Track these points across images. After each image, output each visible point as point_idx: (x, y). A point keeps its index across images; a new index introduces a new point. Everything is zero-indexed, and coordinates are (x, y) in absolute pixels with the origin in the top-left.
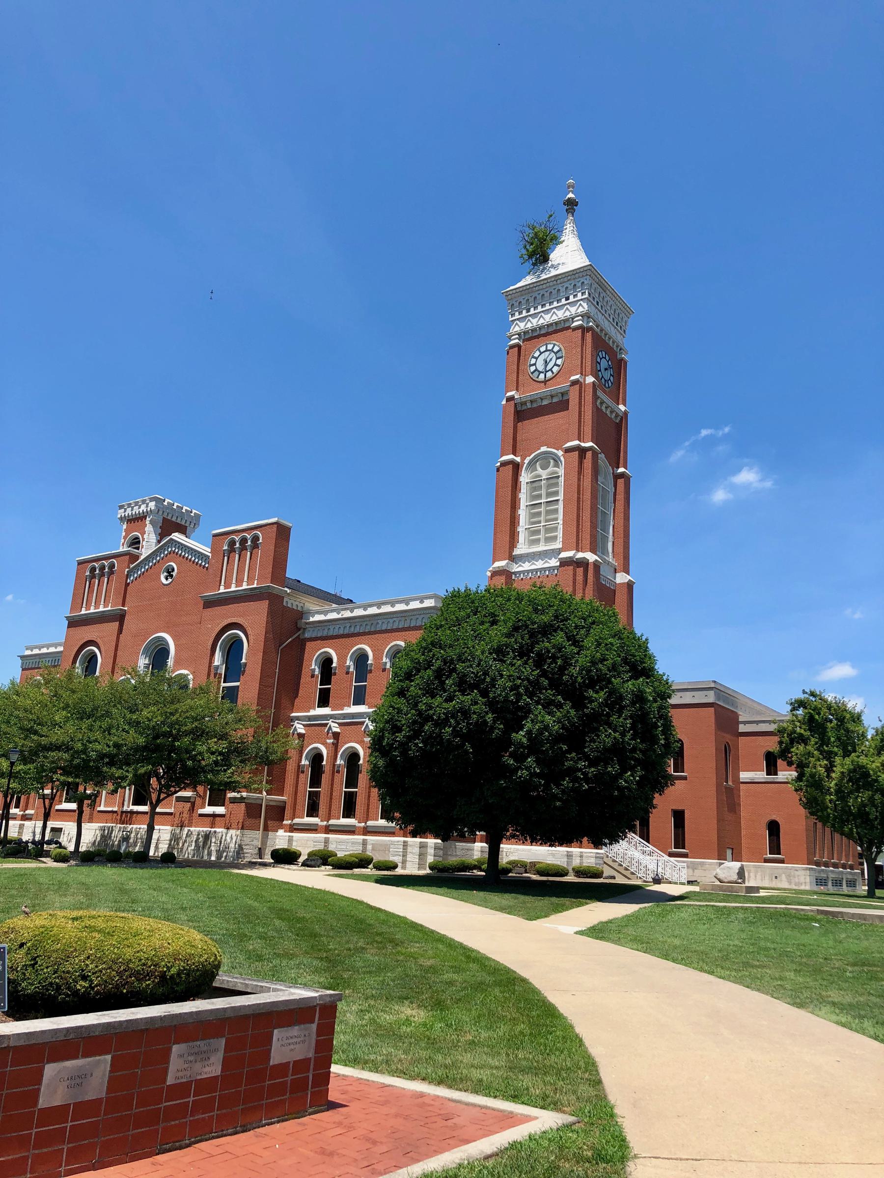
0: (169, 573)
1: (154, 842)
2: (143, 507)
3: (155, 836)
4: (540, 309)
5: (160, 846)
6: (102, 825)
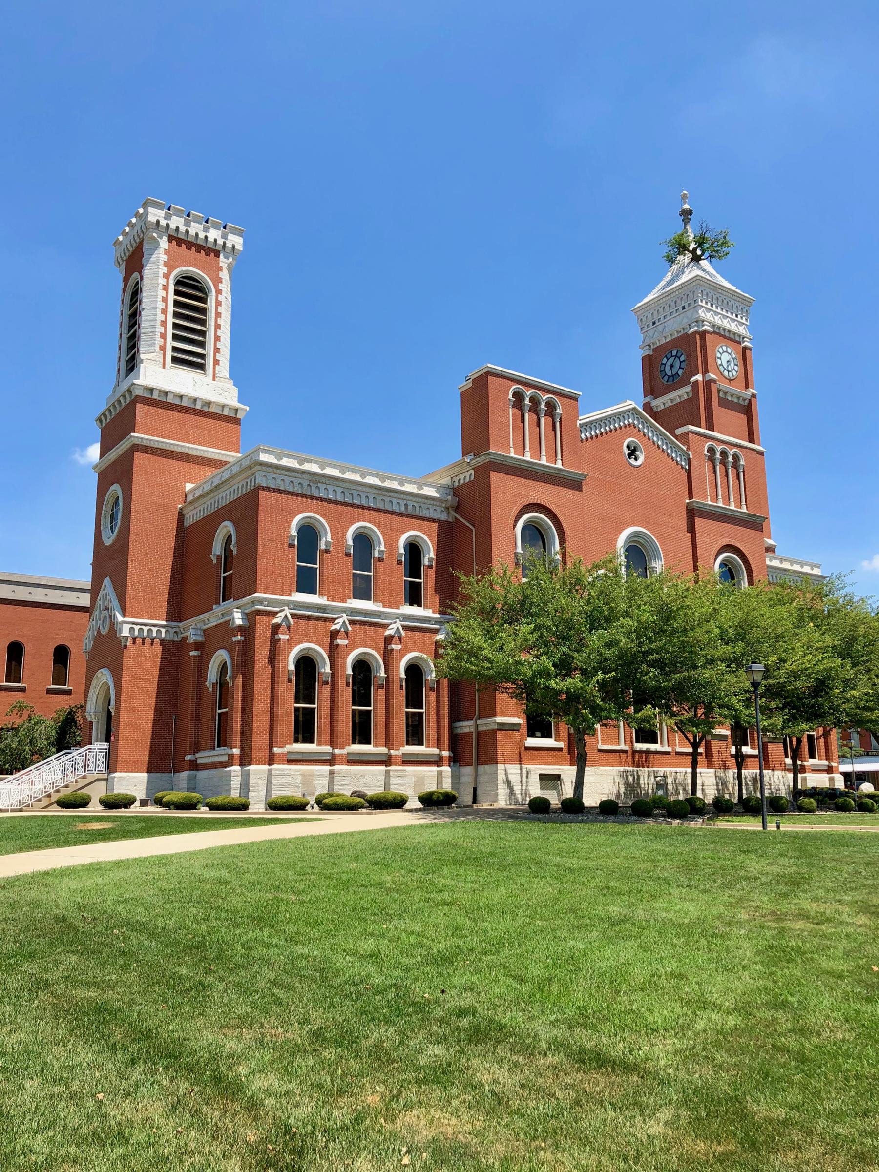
0: (633, 452)
1: (699, 787)
2: (214, 235)
4: (719, 311)
5: (707, 791)
6: (622, 769)
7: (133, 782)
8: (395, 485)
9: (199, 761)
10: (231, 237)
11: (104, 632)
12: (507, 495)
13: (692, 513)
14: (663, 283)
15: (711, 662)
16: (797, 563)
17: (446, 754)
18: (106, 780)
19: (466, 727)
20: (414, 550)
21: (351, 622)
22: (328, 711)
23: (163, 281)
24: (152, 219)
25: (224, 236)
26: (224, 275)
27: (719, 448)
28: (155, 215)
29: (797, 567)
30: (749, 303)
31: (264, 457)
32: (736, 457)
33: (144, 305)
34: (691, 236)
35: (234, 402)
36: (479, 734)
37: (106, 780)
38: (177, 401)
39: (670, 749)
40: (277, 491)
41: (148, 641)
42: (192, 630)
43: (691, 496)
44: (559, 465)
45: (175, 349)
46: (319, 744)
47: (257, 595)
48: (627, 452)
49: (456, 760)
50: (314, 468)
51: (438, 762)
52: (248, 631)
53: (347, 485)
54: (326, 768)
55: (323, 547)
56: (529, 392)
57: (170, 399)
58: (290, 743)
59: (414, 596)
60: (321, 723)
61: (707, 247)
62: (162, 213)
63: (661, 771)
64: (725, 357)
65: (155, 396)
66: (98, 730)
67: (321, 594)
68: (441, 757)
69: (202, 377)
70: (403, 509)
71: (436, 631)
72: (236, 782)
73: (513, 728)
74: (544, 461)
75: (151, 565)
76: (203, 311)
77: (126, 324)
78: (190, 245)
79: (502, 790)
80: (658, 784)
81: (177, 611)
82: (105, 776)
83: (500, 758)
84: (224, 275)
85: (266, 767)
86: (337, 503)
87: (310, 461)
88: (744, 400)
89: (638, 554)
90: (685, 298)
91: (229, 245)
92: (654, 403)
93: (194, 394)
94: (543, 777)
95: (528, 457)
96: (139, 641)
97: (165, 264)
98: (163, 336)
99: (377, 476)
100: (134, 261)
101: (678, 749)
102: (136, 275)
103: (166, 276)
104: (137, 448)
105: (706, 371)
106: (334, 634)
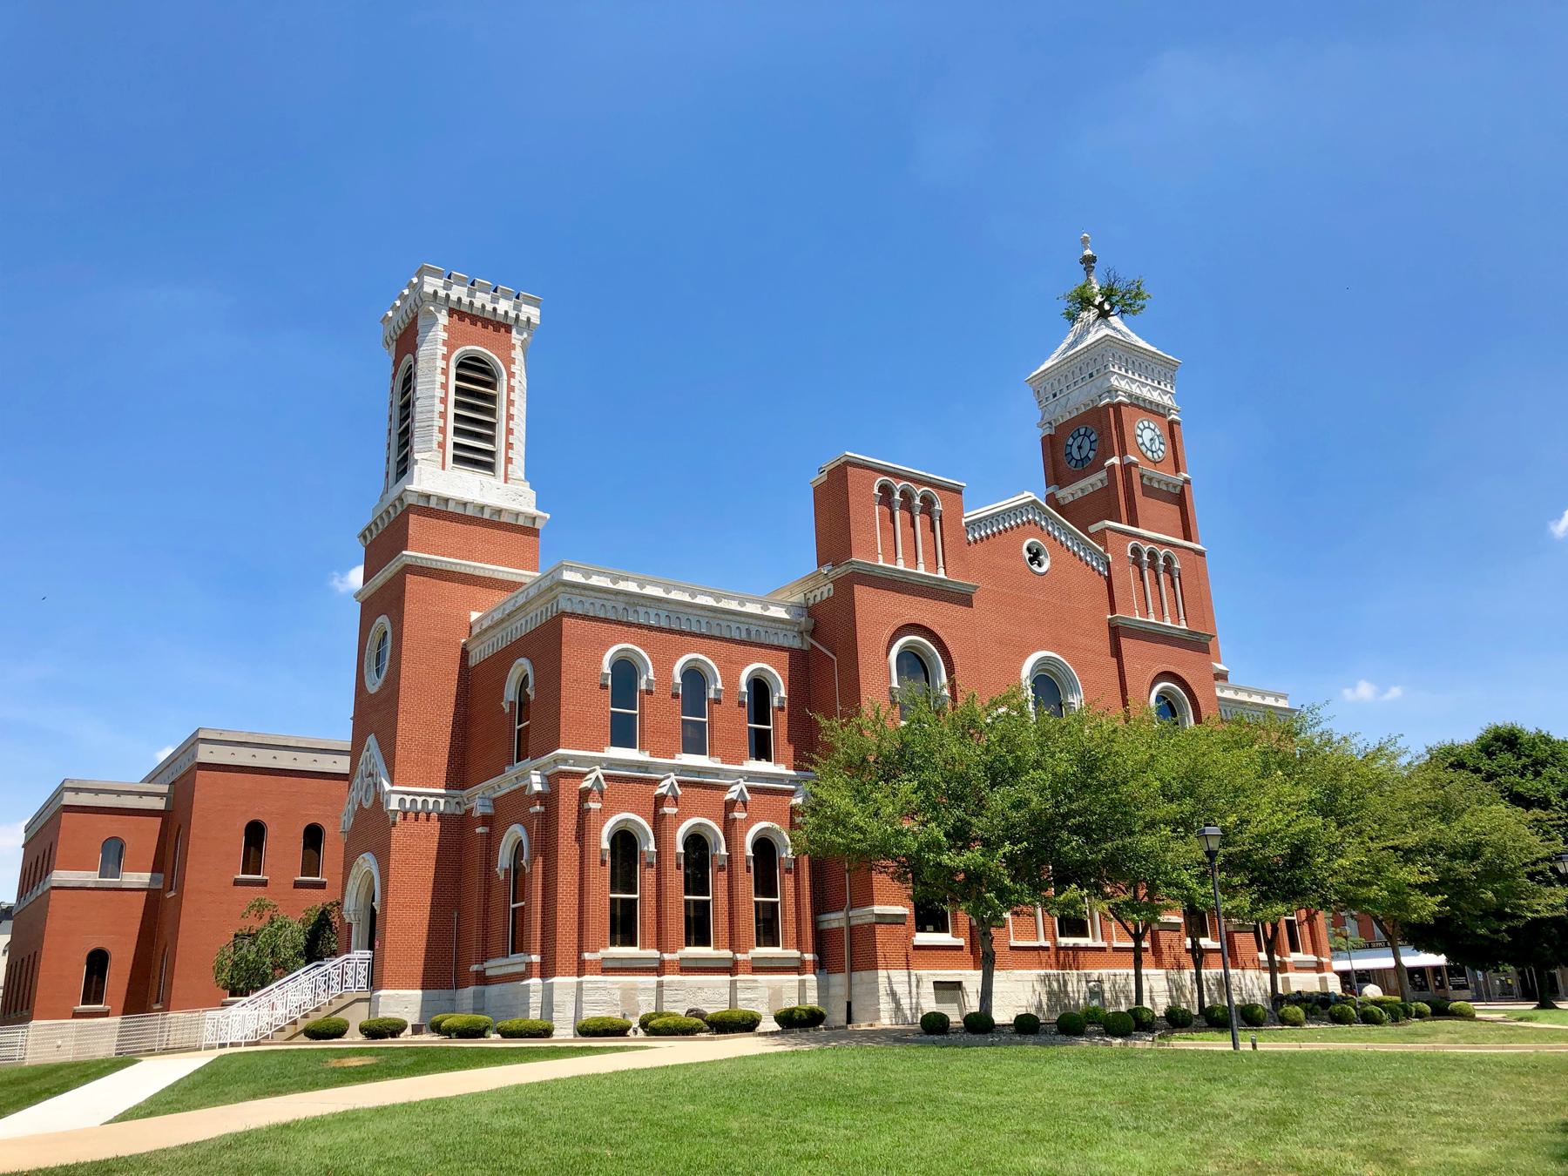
0: (1035, 557)
1: (1146, 994)
2: (504, 306)
3: (1145, 987)
6: (1043, 972)
7: (403, 1002)
8: (733, 605)
9: (489, 973)
10: (525, 308)
11: (367, 805)
12: (876, 614)
13: (1116, 632)
14: (1063, 346)
15: (1152, 825)
16: (1257, 693)
17: (809, 957)
18: (368, 1000)
19: (835, 920)
20: (760, 688)
21: (681, 783)
22: (653, 903)
23: (441, 364)
24: (428, 289)
25: (517, 308)
26: (518, 354)
27: (1146, 548)
28: (432, 284)
29: (1256, 699)
30: (1173, 366)
31: (568, 576)
32: (1168, 559)
33: (418, 394)
34: (1097, 287)
35: (531, 509)
36: (852, 929)
37: (368, 1000)
38: (460, 511)
39: (1105, 944)
40: (585, 617)
41: (422, 816)
42: (479, 800)
43: (1113, 611)
44: (941, 574)
45: (456, 446)
46: (643, 947)
47: (560, 751)
48: (1027, 556)
49: (823, 965)
50: (632, 587)
51: (799, 968)
52: (549, 799)
53: (673, 607)
54: (652, 980)
55: (643, 687)
56: (900, 485)
57: (451, 507)
58: (605, 947)
59: (761, 748)
60: (645, 918)
61: (1118, 300)
62: (440, 282)
63: (1095, 973)
64: (1147, 434)
65: (433, 504)
66: (358, 933)
67: (642, 749)
68: (803, 962)
69: (491, 480)
70: (744, 636)
71: (791, 793)
72: (535, 999)
73: (897, 920)
74: (921, 570)
75: (427, 717)
76: (492, 399)
77: (396, 417)
78: (474, 319)
79: (885, 1005)
80: (1091, 991)
81: (459, 775)
82: (368, 995)
83: (881, 961)
84: (518, 354)
85: (575, 979)
86: (661, 630)
87: (627, 579)
88: (1175, 487)
89: (1048, 686)
90: (1094, 362)
91: (523, 317)
92: (1060, 494)
93: (480, 500)
94: (938, 985)
95: (901, 566)
96: (411, 815)
97: (445, 343)
98: (443, 430)
99: (711, 595)
100: (407, 341)
101: (1116, 944)
102: (409, 357)
103: (446, 358)
104: (411, 569)
105: (1123, 453)
106: (660, 801)
